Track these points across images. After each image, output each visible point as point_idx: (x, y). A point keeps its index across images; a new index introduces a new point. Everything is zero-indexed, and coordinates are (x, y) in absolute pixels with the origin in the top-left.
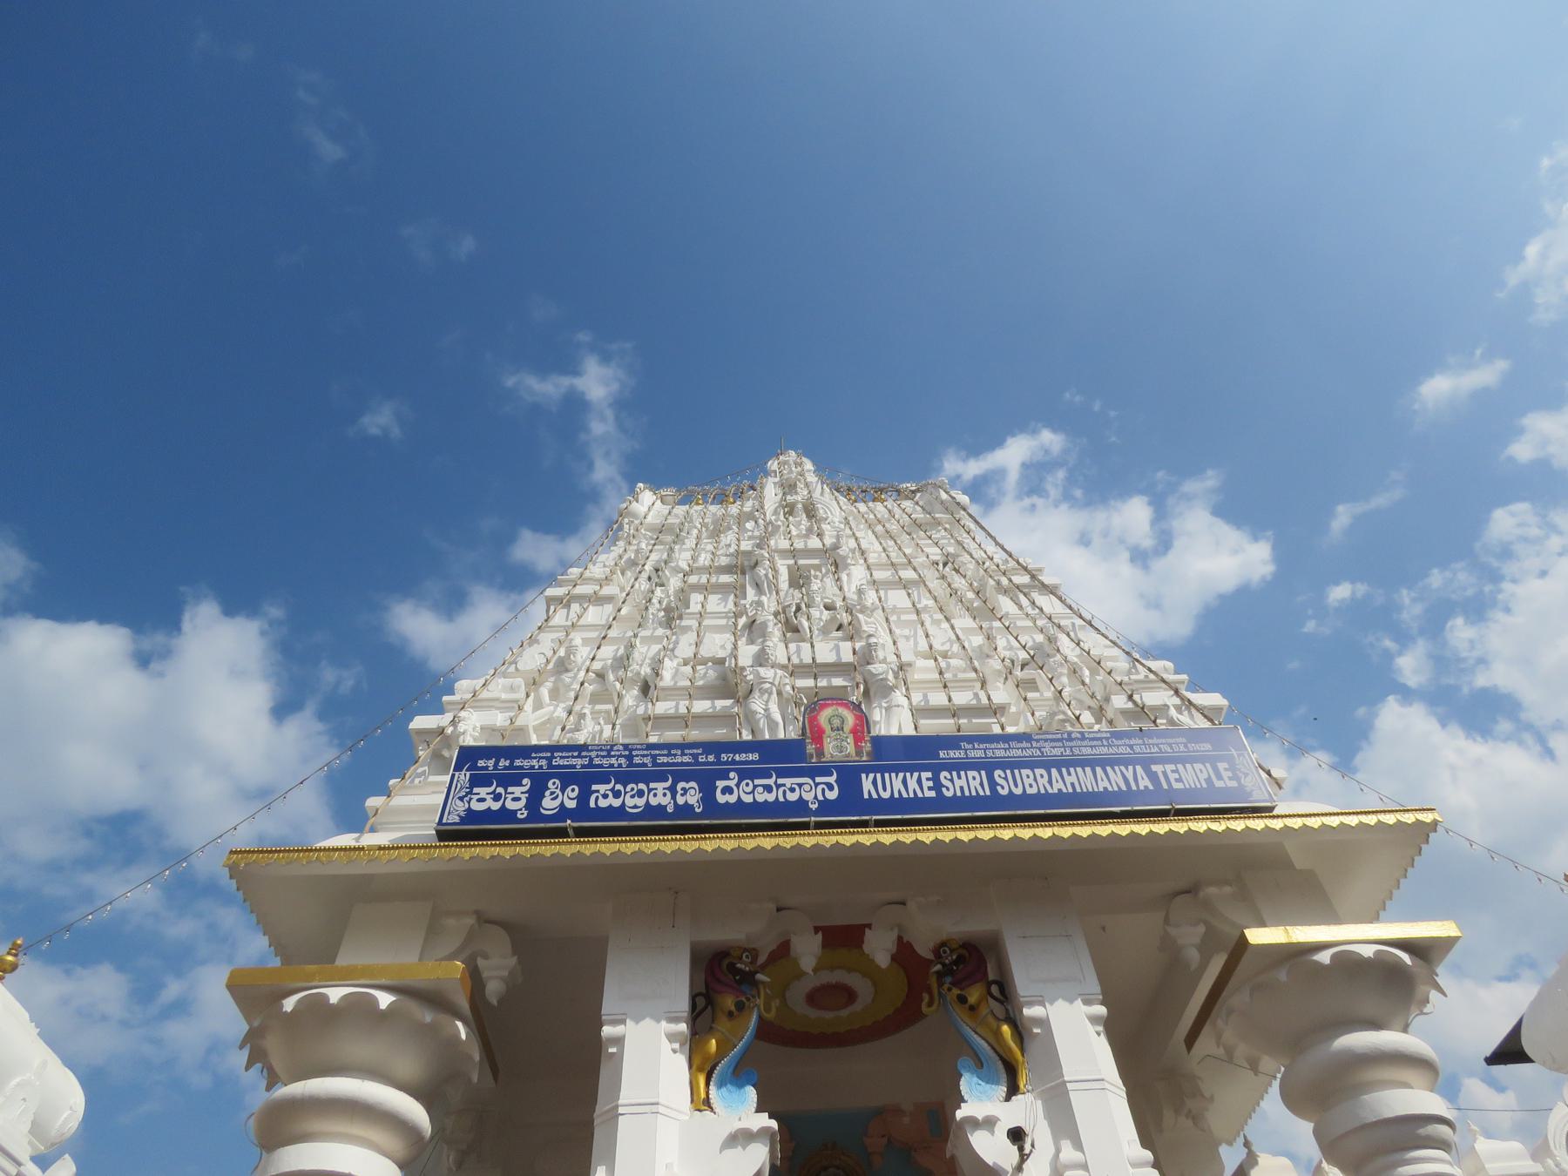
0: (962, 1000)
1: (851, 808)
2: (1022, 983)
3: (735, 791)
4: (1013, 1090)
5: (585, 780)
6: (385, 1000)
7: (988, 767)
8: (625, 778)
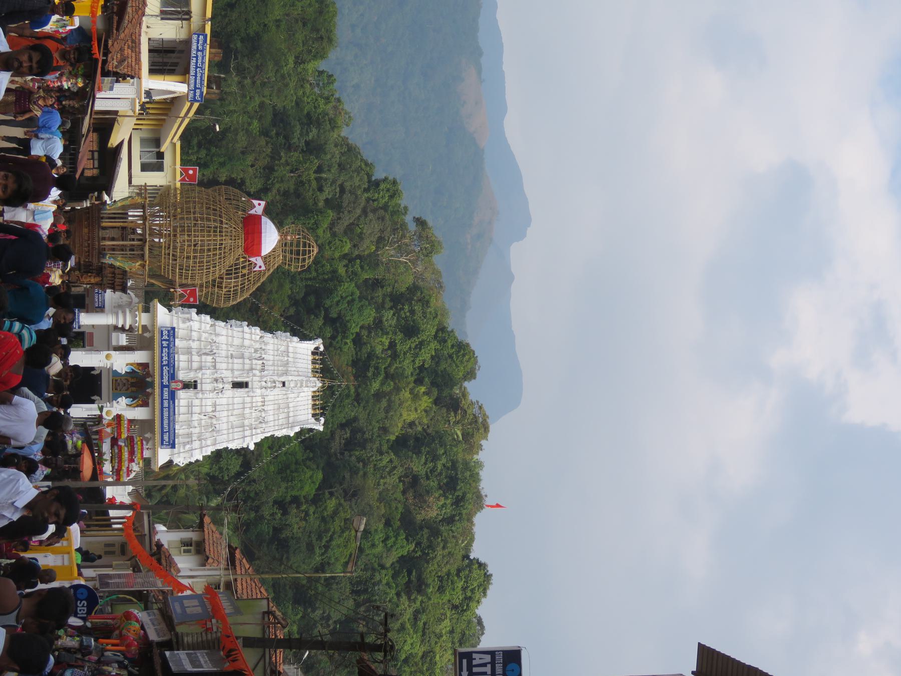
1: (163, 386)
2: (140, 408)
3: (165, 369)
5: (168, 347)
7: (169, 407)
8: (168, 353)
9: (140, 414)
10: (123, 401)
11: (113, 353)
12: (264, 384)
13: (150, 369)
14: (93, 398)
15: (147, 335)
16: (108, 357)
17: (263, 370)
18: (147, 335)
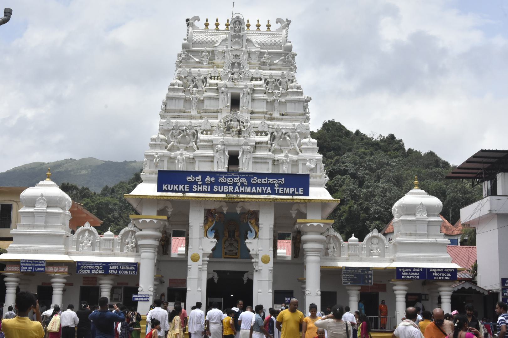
0: (250, 222)
2: (261, 222)
4: (255, 237)
6: (155, 221)
9: (267, 223)
10: (252, 244)
11: (190, 253)
12: (235, 76)
13: (212, 207)
14: (245, 281)
15: (170, 211)
16: (195, 259)
17: (218, 78)
18: (170, 211)
